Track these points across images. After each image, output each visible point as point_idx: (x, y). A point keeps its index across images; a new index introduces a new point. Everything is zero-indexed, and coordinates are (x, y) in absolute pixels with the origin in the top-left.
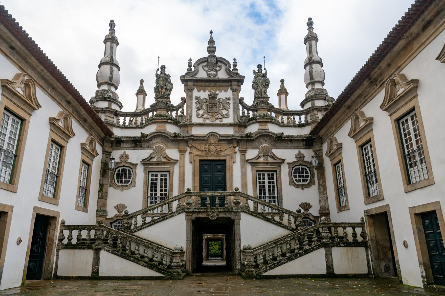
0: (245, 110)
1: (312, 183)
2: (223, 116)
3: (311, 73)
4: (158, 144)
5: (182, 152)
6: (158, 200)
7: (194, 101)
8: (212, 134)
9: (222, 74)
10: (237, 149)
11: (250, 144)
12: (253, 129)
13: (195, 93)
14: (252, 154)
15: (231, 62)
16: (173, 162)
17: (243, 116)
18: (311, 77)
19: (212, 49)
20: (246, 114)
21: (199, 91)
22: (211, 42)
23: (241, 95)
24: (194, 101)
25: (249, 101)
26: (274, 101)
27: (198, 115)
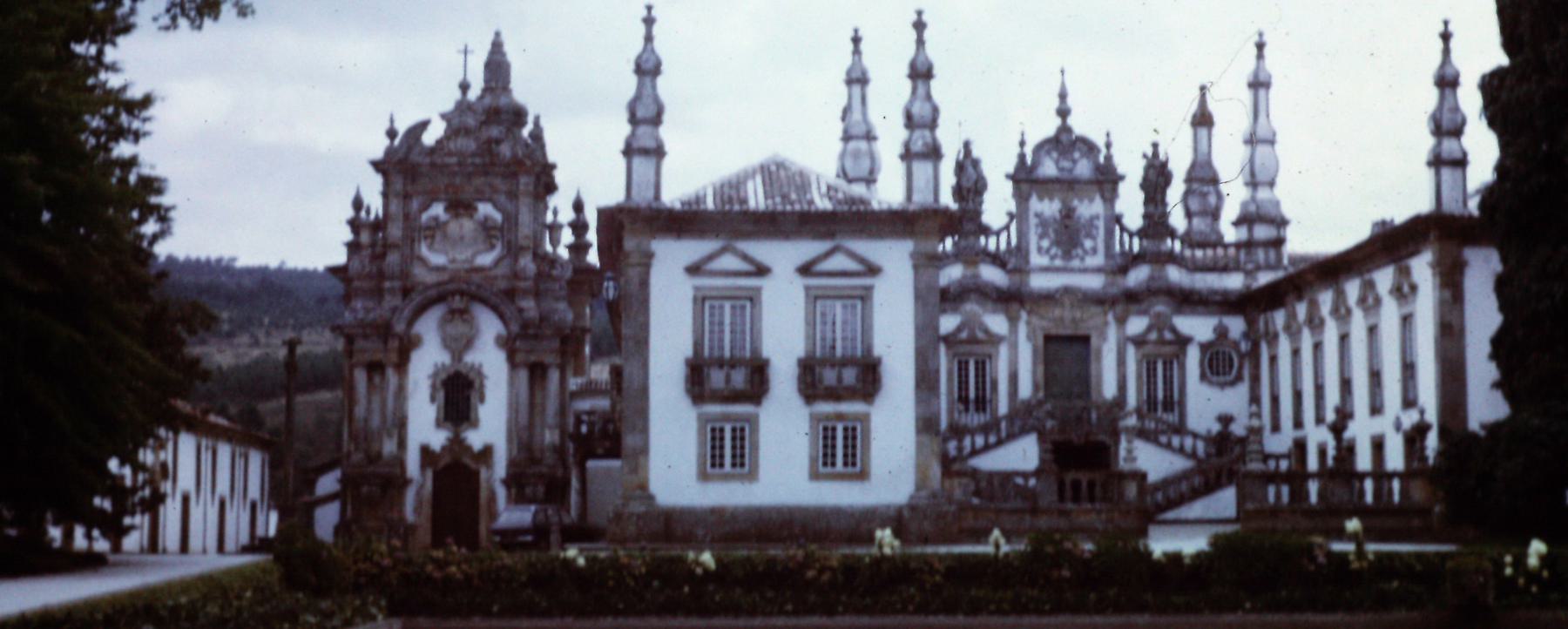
0: (1126, 237)
1: (1239, 378)
2: (1086, 252)
3: (1252, 161)
4: (971, 307)
5: (1013, 321)
6: (972, 407)
7: (1033, 221)
8: (1067, 290)
9: (1083, 168)
10: (1110, 317)
11: (1133, 308)
12: (1138, 276)
13: (1036, 205)
14: (1137, 325)
15: (1100, 141)
16: (995, 340)
17: (1123, 253)
18: (1253, 174)
19: (1063, 113)
20: (1127, 247)
21: (1041, 199)
22: (1063, 96)
23: (1120, 206)
24: (1033, 221)
25: (1134, 219)
26: (1178, 220)
27: (1040, 249)
